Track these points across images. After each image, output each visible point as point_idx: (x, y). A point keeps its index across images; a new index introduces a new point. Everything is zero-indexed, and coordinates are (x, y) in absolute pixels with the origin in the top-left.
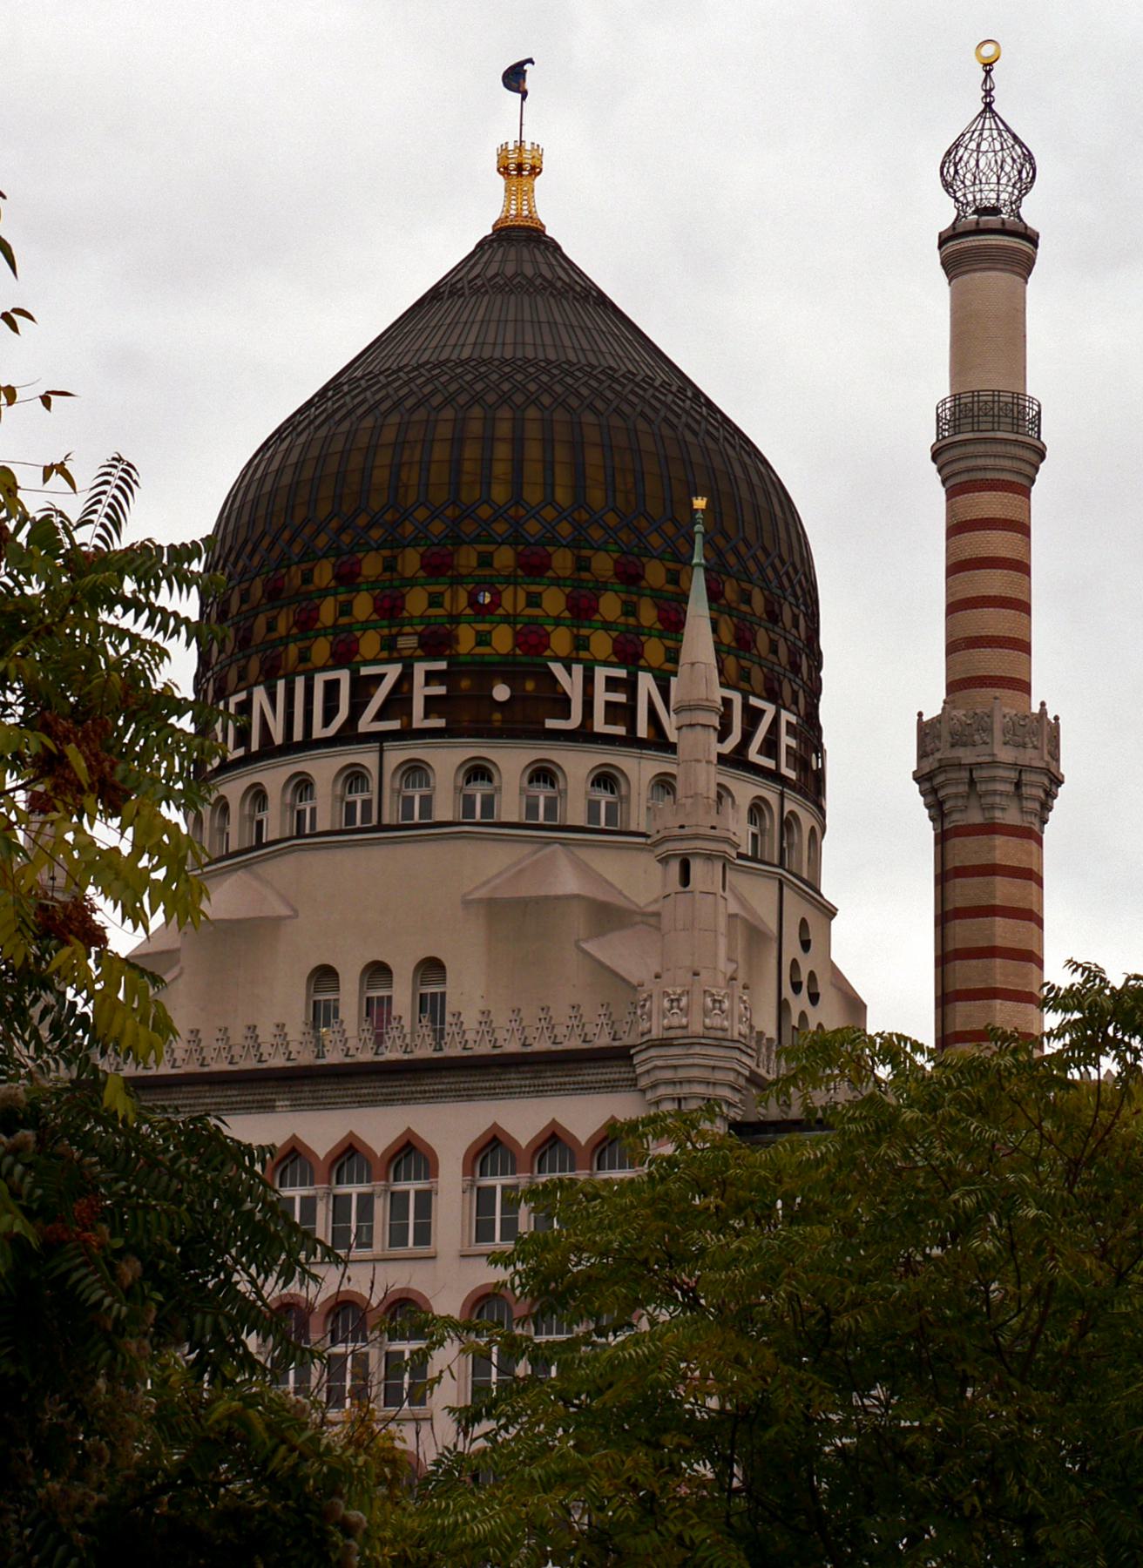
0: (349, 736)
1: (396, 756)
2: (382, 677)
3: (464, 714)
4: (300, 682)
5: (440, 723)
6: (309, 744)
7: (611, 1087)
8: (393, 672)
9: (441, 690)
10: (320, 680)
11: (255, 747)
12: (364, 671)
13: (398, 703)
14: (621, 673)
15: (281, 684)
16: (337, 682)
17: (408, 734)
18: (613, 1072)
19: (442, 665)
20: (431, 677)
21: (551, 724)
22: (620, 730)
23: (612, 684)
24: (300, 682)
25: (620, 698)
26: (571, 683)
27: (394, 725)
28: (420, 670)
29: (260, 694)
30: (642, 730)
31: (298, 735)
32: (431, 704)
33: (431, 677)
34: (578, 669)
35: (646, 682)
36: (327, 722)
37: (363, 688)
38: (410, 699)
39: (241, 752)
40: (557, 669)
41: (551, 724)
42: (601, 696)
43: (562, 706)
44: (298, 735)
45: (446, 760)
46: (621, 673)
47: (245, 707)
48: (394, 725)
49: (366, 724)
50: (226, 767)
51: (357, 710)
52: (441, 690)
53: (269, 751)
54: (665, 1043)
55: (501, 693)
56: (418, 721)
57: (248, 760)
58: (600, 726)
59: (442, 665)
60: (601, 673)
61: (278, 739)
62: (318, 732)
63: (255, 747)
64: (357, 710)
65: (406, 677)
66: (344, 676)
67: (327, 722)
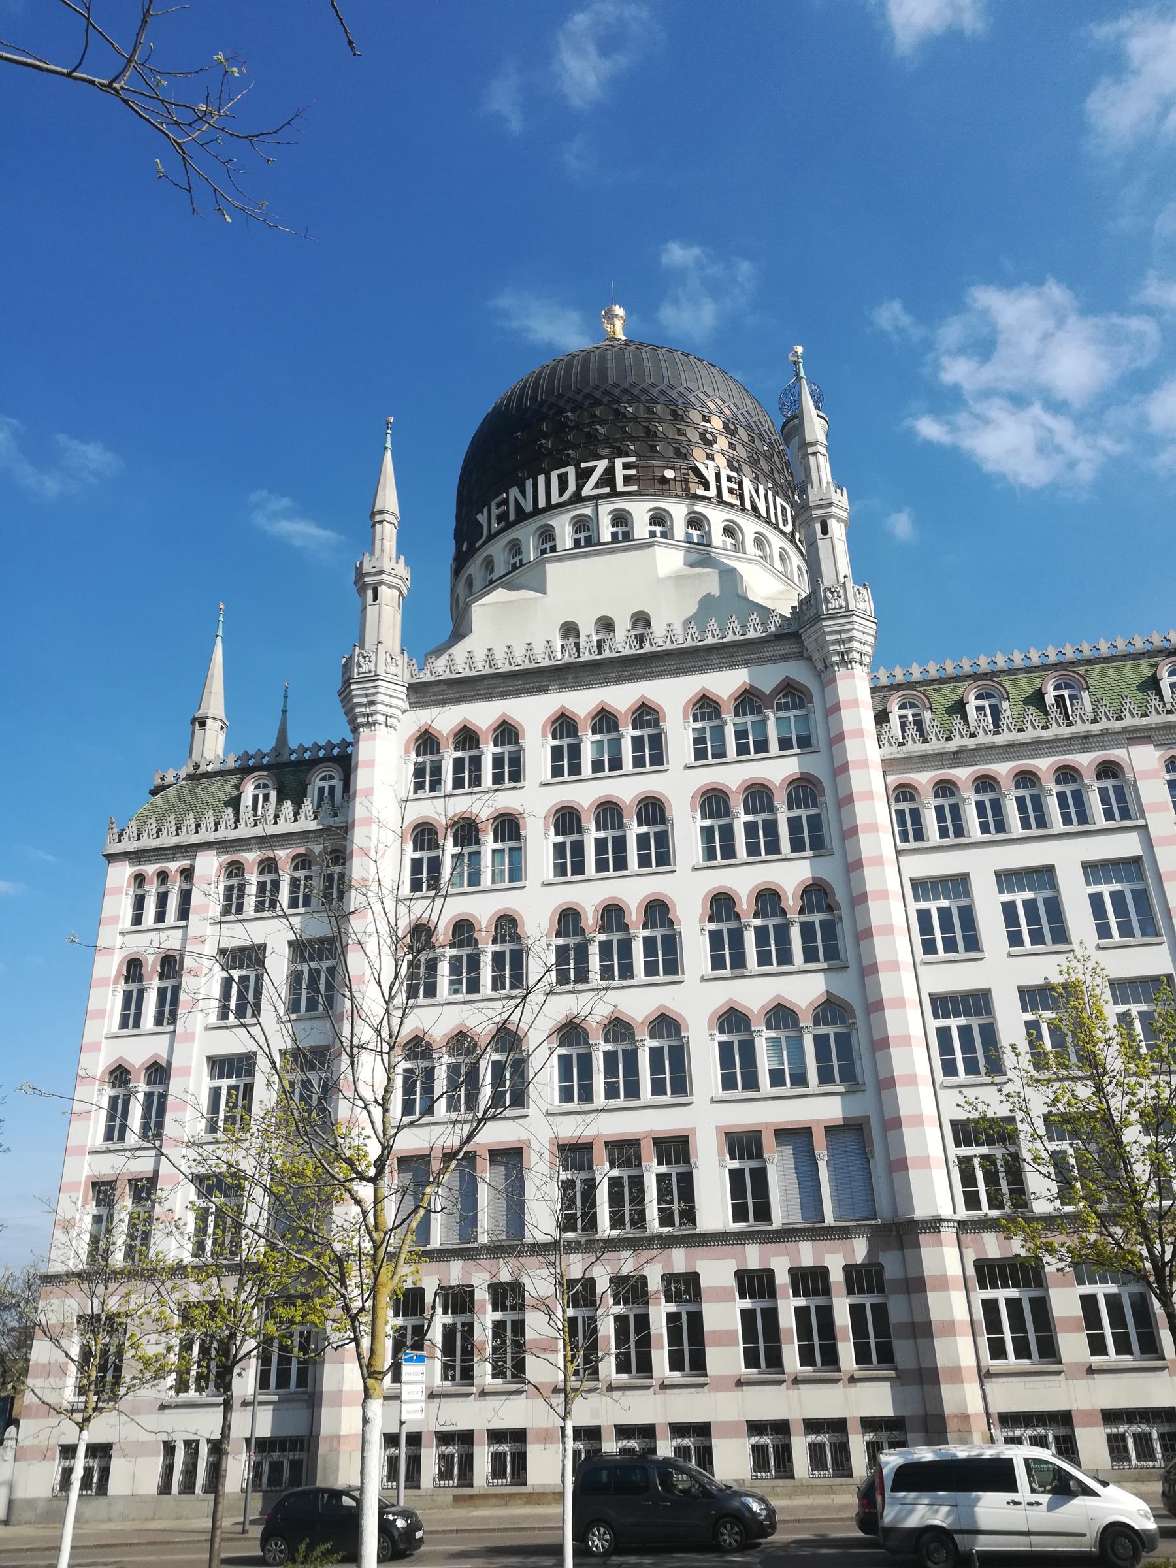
0: (578, 498)
1: (605, 510)
2: (592, 469)
3: (648, 483)
4: (541, 479)
5: (635, 488)
6: (550, 507)
7: (784, 658)
8: (602, 465)
9: (633, 472)
10: (554, 475)
11: (512, 517)
12: (583, 465)
13: (608, 478)
15: (529, 483)
16: (566, 473)
17: (614, 494)
18: (787, 648)
19: (633, 459)
20: (626, 466)
23: (729, 479)
24: (541, 479)
27: (607, 490)
28: (619, 462)
29: (514, 492)
30: (748, 506)
31: (542, 503)
32: (627, 480)
33: (626, 466)
35: (747, 483)
36: (560, 495)
37: (583, 476)
38: (614, 478)
39: (503, 524)
42: (725, 484)
44: (542, 503)
45: (640, 510)
47: (506, 502)
48: (607, 490)
49: (587, 491)
50: (491, 537)
51: (580, 487)
52: (634, 472)
53: (522, 516)
54: (832, 617)
56: (620, 486)
57: (510, 525)
58: (726, 497)
59: (633, 459)
61: (528, 507)
62: (555, 499)
63: (512, 517)
64: (580, 487)
65: (610, 470)
66: (571, 471)
67: (560, 495)
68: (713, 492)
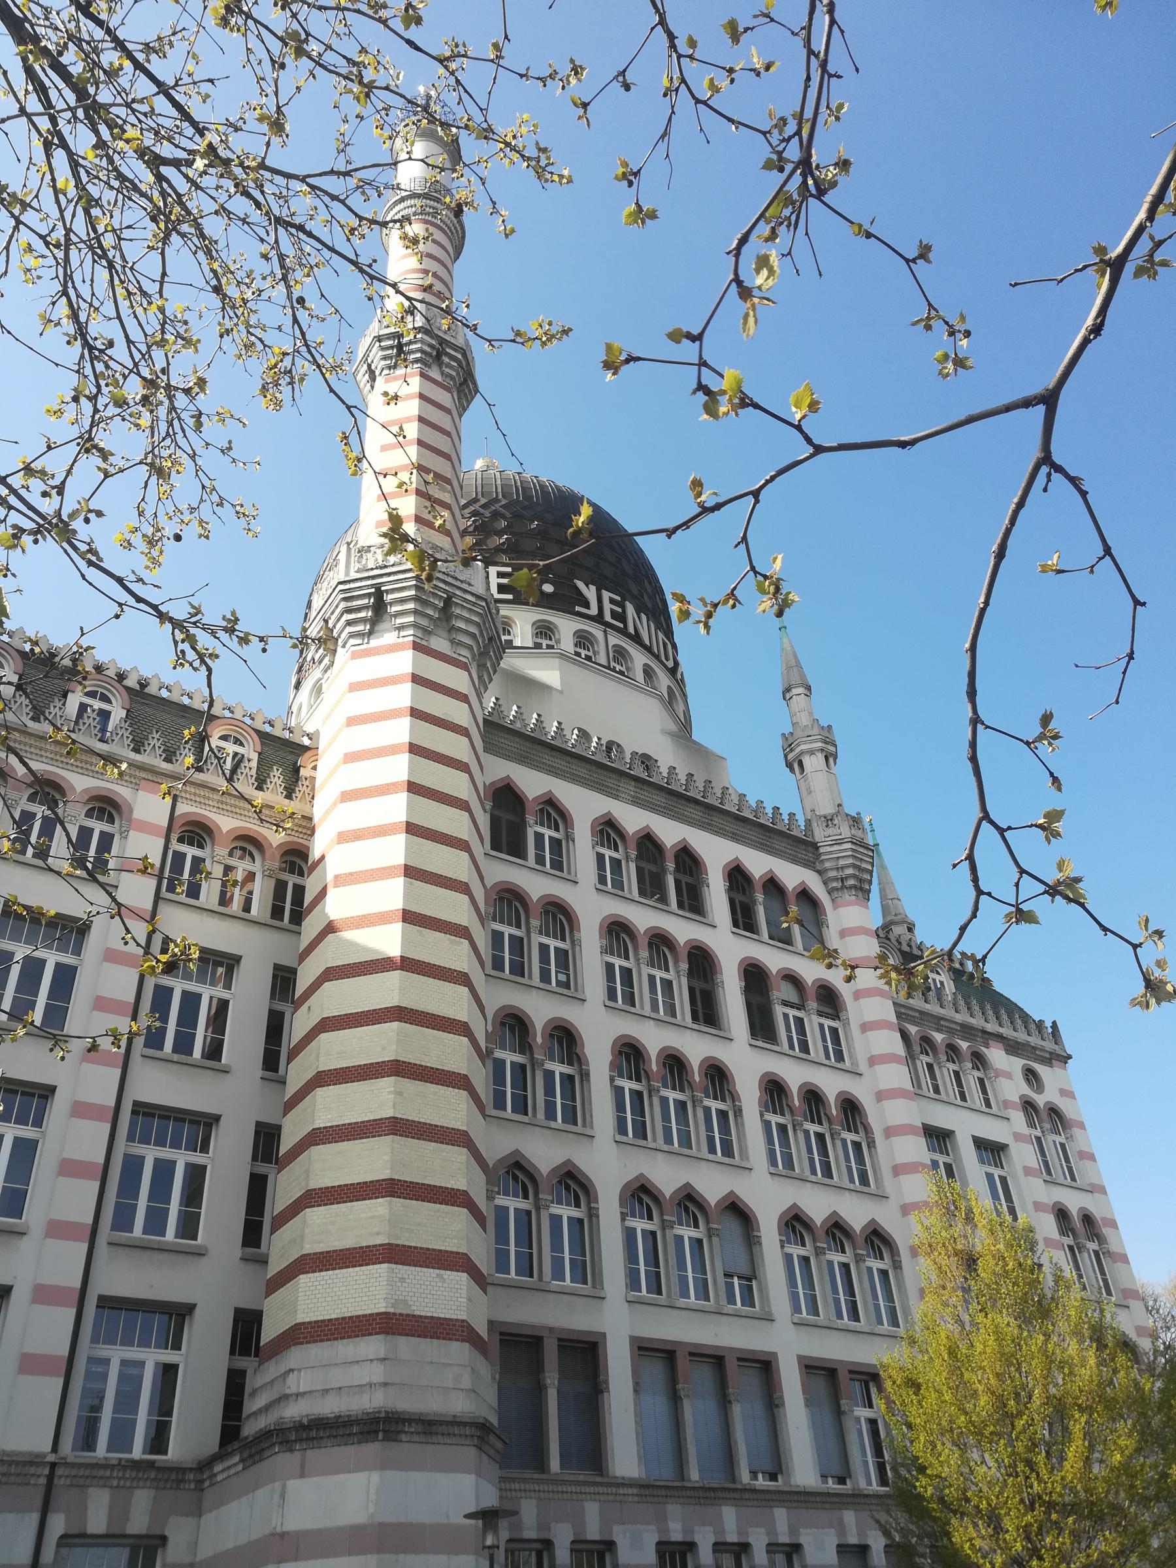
9: (505, 581)
14: (619, 598)
21: (577, 608)
22: (621, 625)
23: (612, 601)
25: (620, 610)
26: (590, 593)
30: (631, 630)
34: (593, 588)
40: (580, 585)
41: (577, 608)
43: (587, 605)
46: (619, 598)
55: (548, 588)
58: (608, 617)
60: (606, 595)
68: (594, 611)
